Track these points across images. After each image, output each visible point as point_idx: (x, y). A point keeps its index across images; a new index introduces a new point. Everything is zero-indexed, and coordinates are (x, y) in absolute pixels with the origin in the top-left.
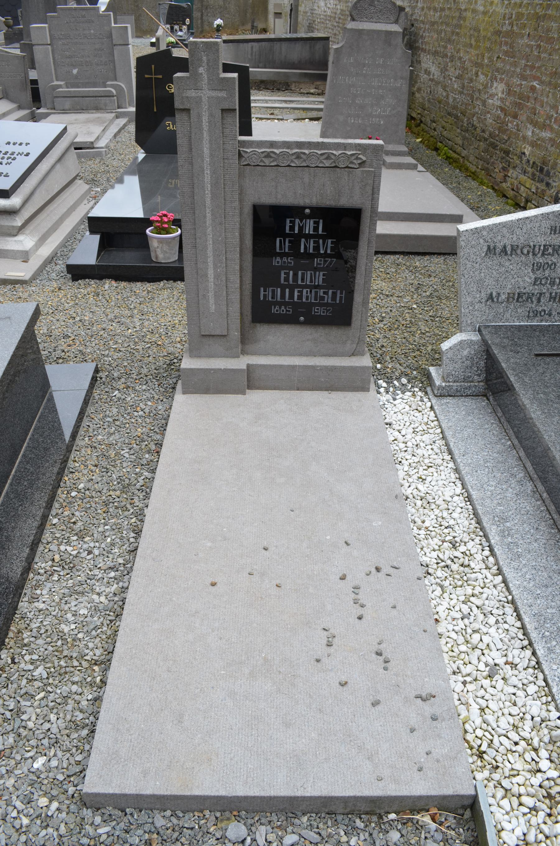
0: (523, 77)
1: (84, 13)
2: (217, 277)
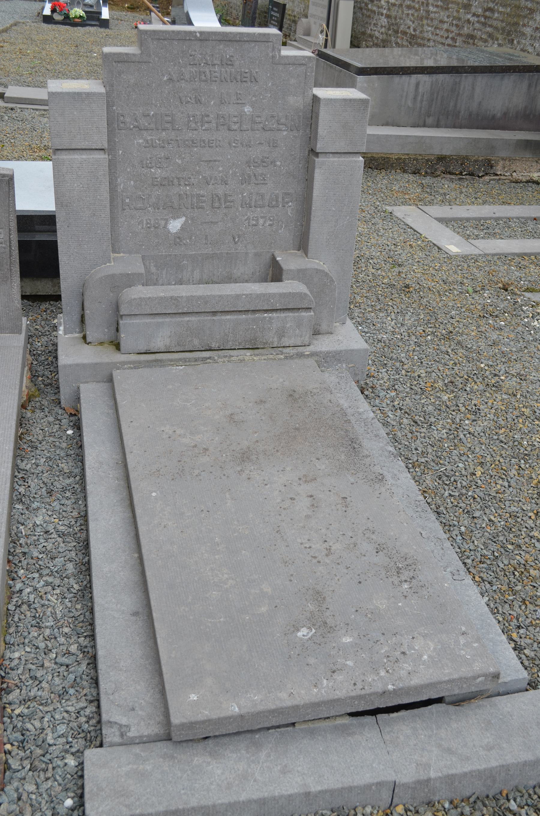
1: (229, 51)
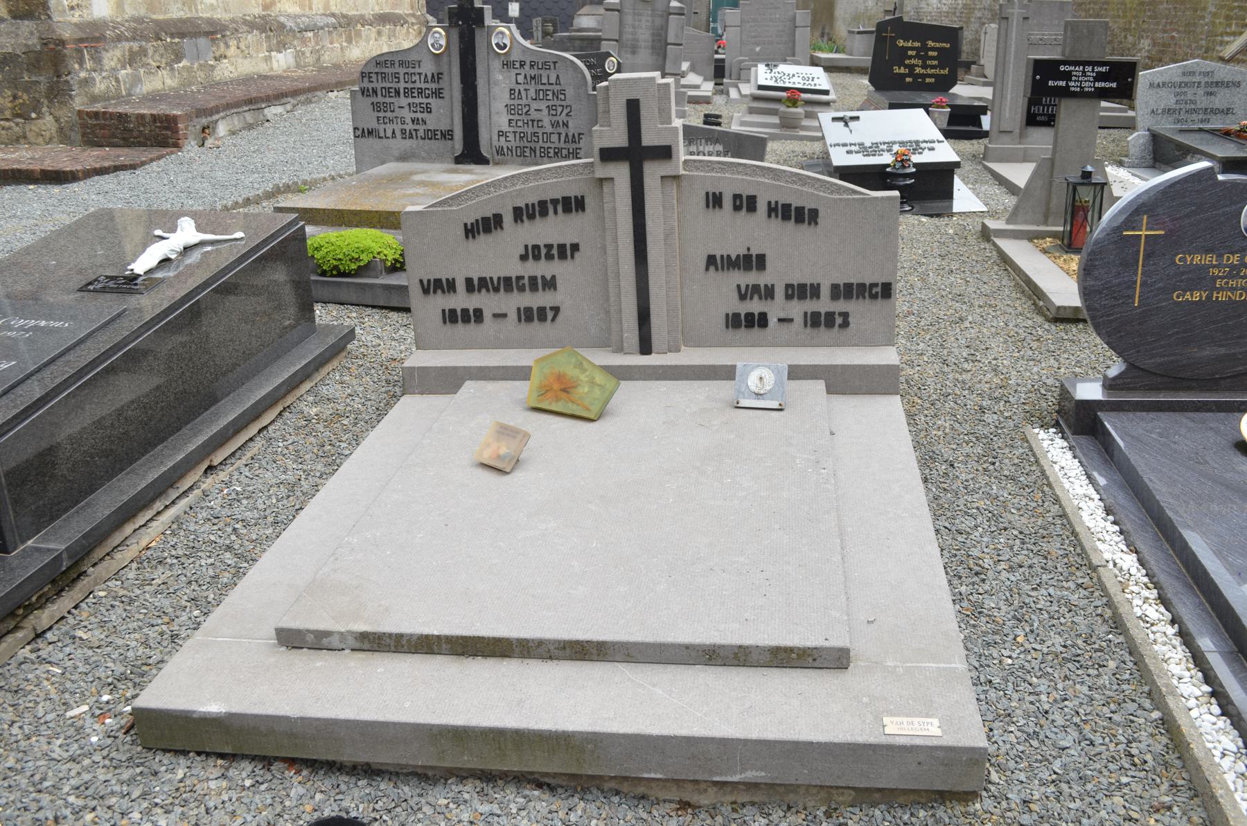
0: (1165, 31)
2: (1011, 99)
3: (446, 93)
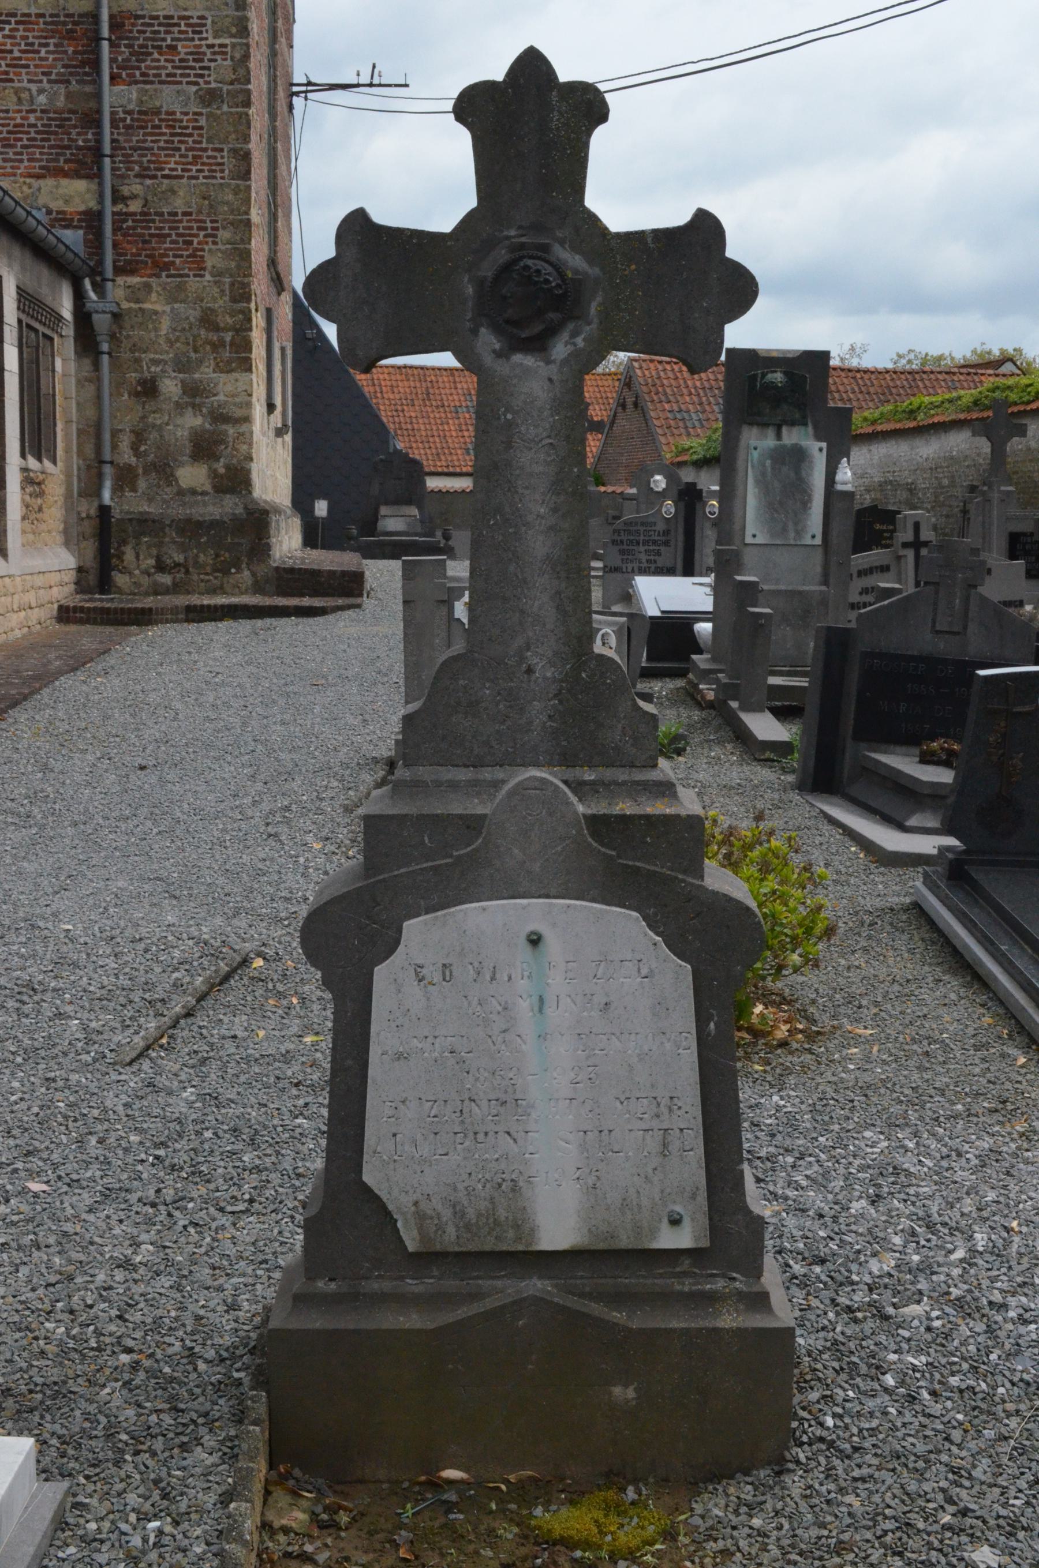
3: (672, 543)
